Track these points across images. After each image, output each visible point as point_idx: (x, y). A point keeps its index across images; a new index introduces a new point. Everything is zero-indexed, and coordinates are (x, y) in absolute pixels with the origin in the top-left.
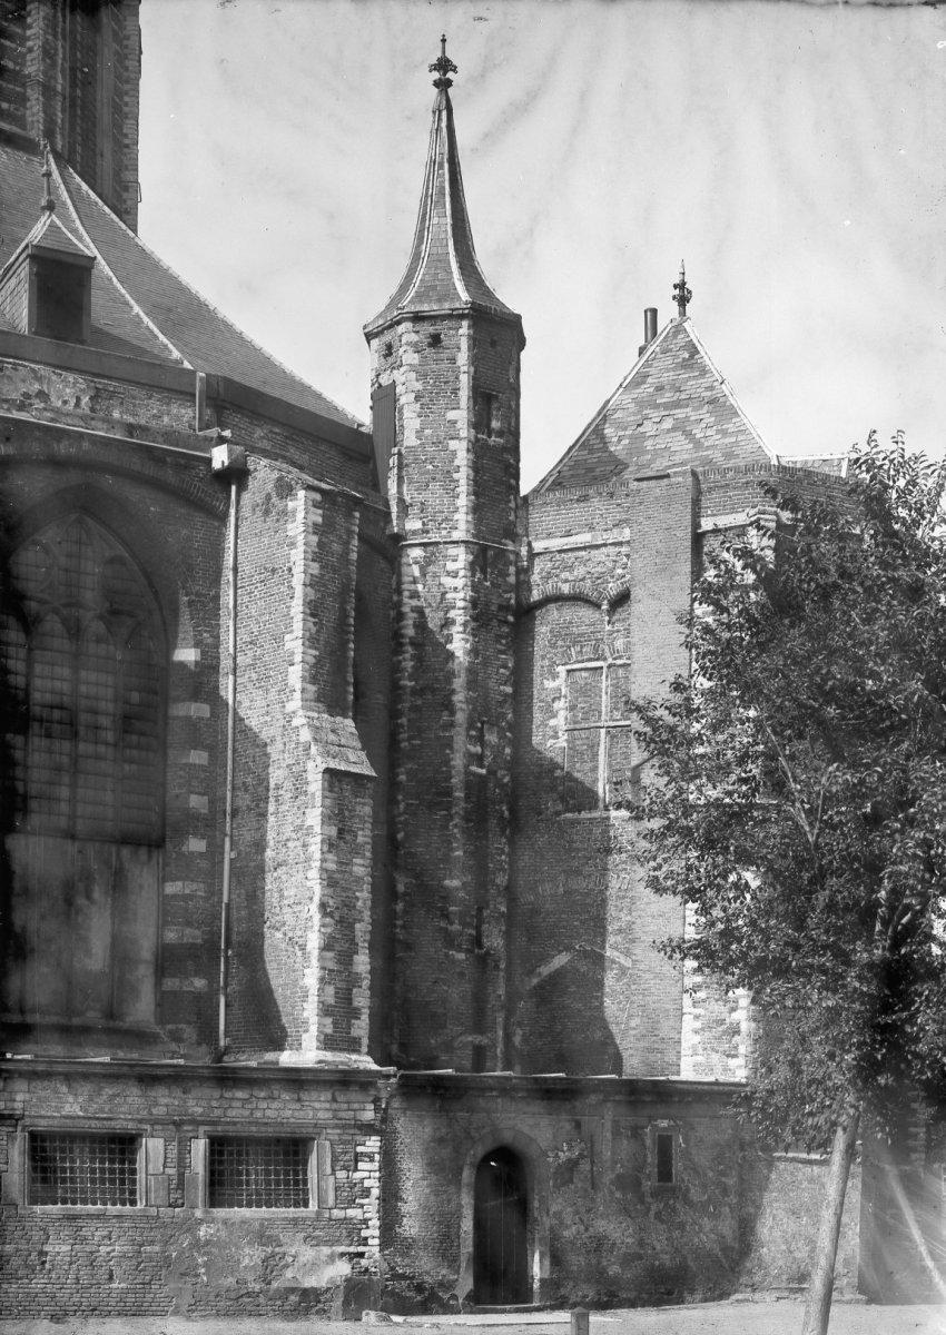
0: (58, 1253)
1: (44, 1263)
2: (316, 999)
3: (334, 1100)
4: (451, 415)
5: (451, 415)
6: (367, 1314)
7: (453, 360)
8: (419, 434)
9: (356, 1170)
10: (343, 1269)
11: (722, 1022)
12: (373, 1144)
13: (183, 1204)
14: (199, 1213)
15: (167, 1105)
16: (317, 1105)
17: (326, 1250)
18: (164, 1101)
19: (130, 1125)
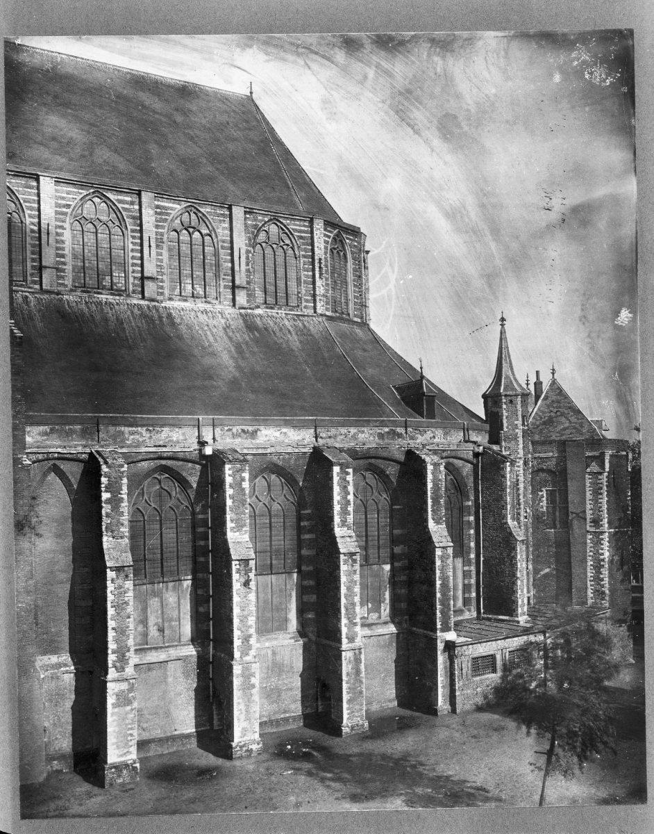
4: (516, 422)
5: (516, 422)
7: (516, 407)
8: (507, 427)
11: (598, 591)
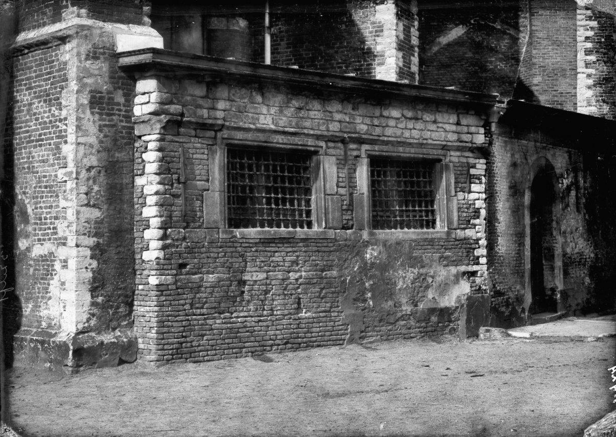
0: (256, 281)
1: (243, 292)
2: (394, 33)
3: (458, 124)
6: (488, 331)
9: (470, 192)
10: (464, 288)
12: (480, 167)
13: (353, 225)
14: (365, 235)
15: (340, 121)
16: (448, 127)
17: (453, 270)
18: (338, 116)
19: (310, 142)
